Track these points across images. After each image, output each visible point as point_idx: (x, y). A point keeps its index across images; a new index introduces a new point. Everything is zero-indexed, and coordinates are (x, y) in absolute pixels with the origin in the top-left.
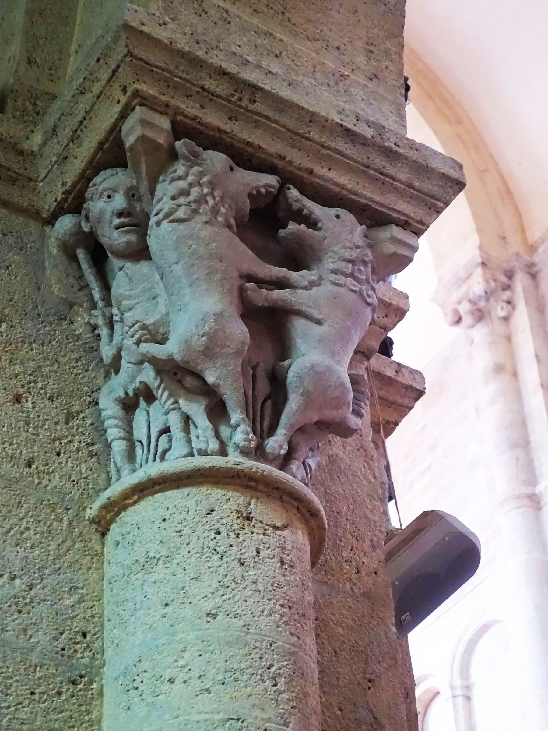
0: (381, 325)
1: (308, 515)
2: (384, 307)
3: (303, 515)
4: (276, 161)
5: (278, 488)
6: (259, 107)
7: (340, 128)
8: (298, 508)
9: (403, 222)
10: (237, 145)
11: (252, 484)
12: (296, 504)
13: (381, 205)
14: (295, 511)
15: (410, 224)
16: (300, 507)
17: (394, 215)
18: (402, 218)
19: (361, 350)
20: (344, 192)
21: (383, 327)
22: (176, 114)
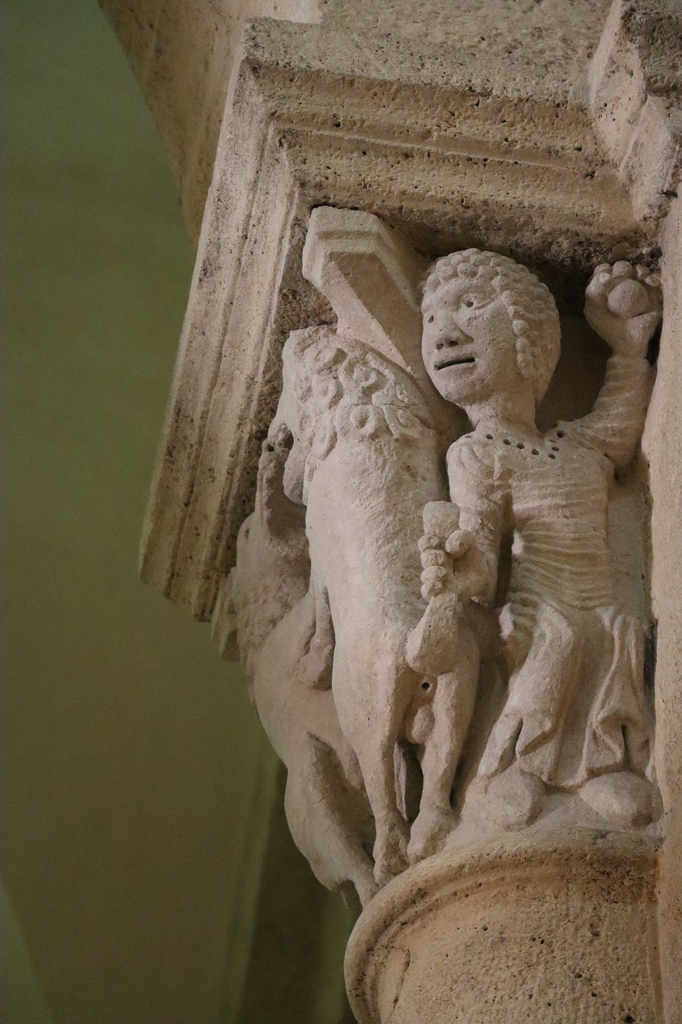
0: (638, 103)
1: (420, 907)
2: (617, 74)
3: (418, 915)
4: (246, 436)
5: (370, 950)
6: (197, 422)
7: (205, 284)
8: (404, 924)
9: (297, 229)
10: (234, 491)
11: (368, 980)
12: (394, 927)
13: (276, 270)
14: (409, 929)
15: (296, 219)
16: (402, 919)
17: (286, 246)
18: (288, 233)
19: (670, 173)
20: (268, 330)
21: (643, 95)
22: (215, 569)
